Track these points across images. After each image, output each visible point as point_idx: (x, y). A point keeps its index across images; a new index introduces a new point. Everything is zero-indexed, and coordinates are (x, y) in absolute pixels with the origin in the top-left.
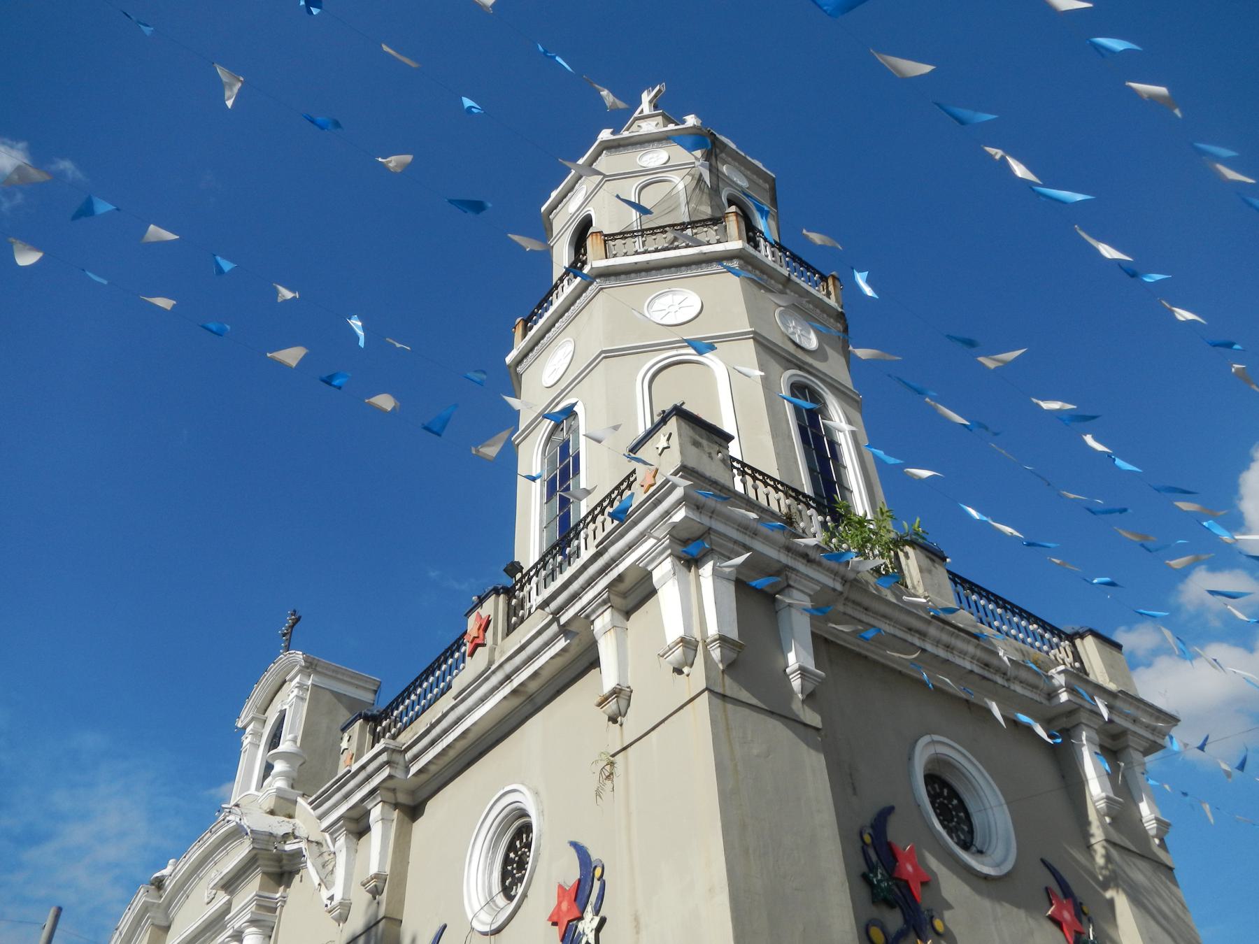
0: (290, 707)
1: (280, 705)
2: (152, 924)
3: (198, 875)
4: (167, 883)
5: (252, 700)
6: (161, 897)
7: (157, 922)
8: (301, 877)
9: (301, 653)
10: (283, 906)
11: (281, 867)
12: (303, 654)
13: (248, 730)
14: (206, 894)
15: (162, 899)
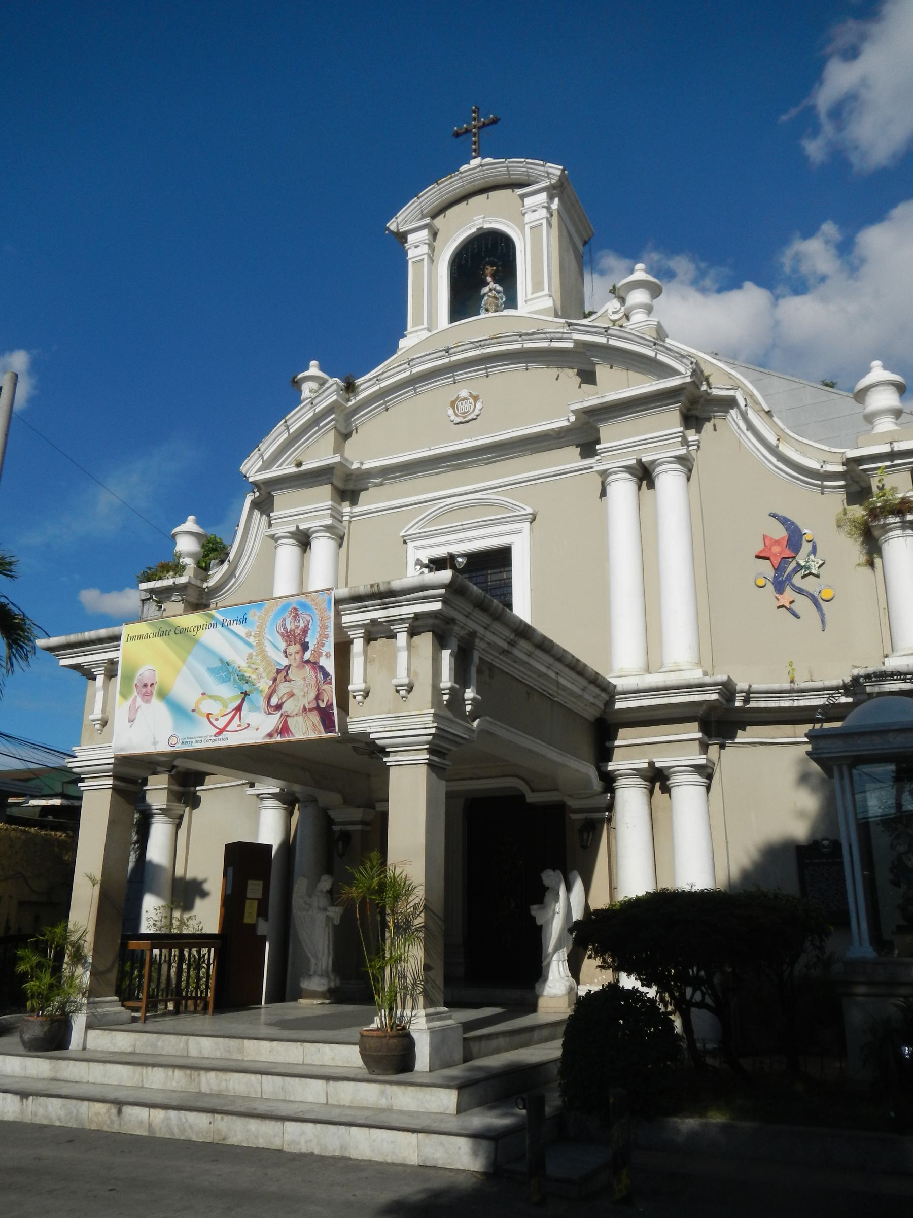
0: (531, 228)
1: (481, 220)
2: (335, 428)
3: (415, 389)
4: (362, 387)
5: (419, 201)
6: (348, 400)
7: (339, 427)
8: (715, 426)
9: (561, 167)
10: (697, 451)
11: (689, 410)
12: (563, 171)
13: (411, 238)
14: (451, 412)
15: (350, 404)
